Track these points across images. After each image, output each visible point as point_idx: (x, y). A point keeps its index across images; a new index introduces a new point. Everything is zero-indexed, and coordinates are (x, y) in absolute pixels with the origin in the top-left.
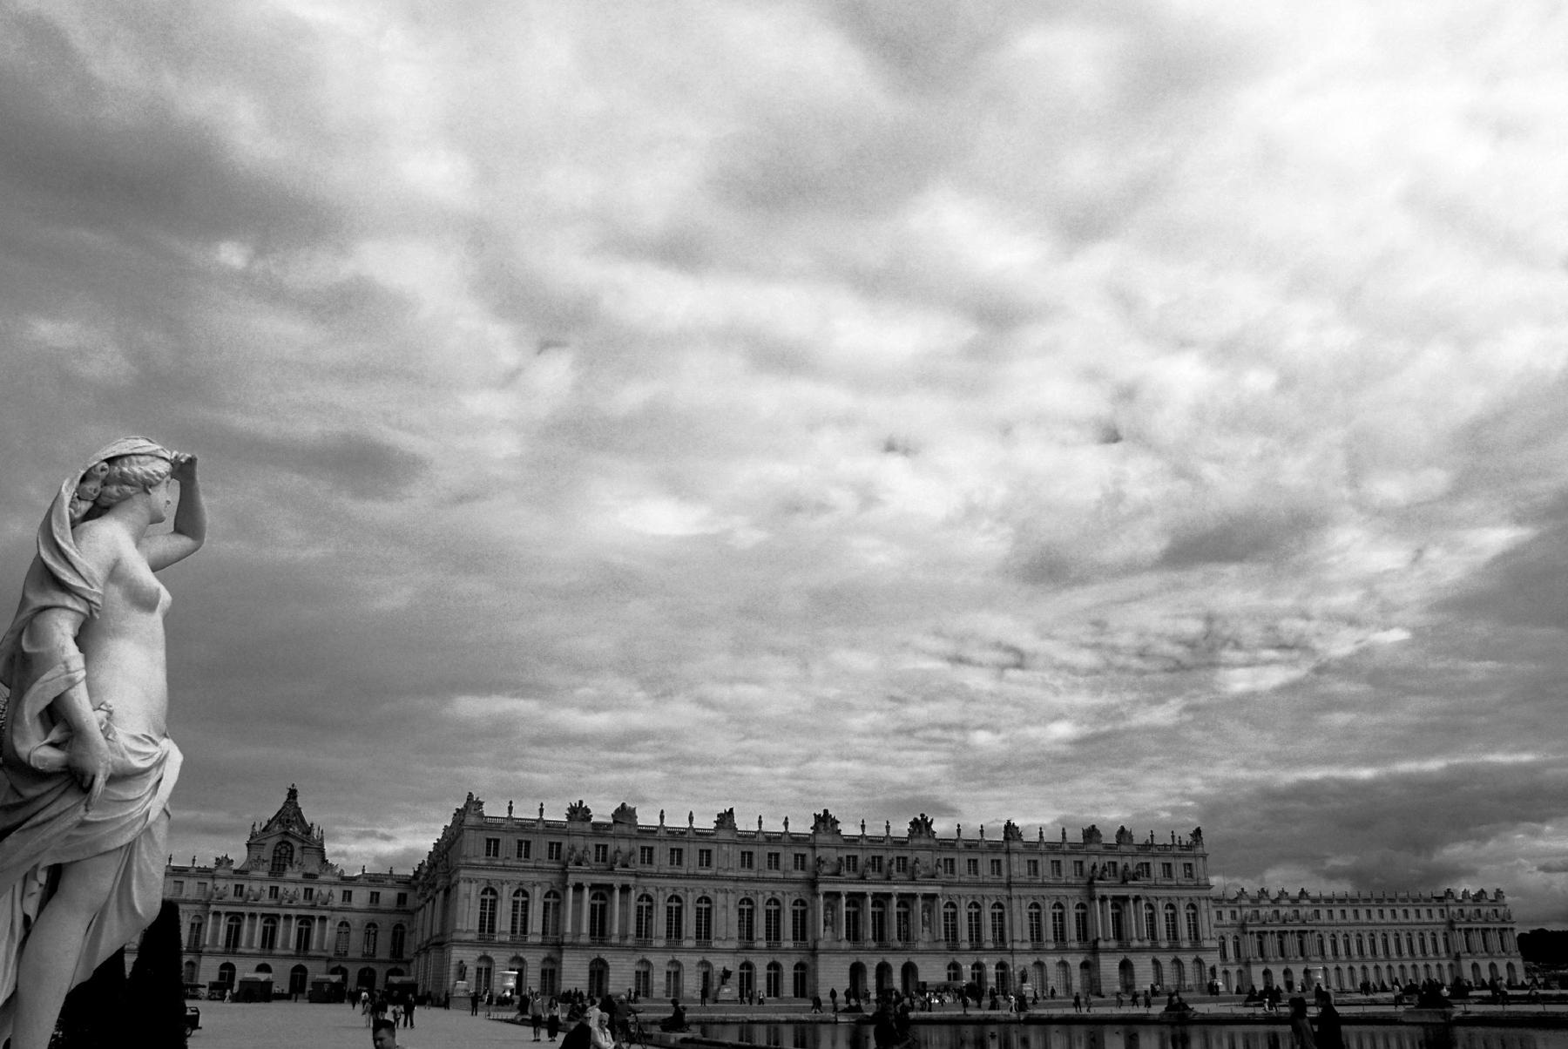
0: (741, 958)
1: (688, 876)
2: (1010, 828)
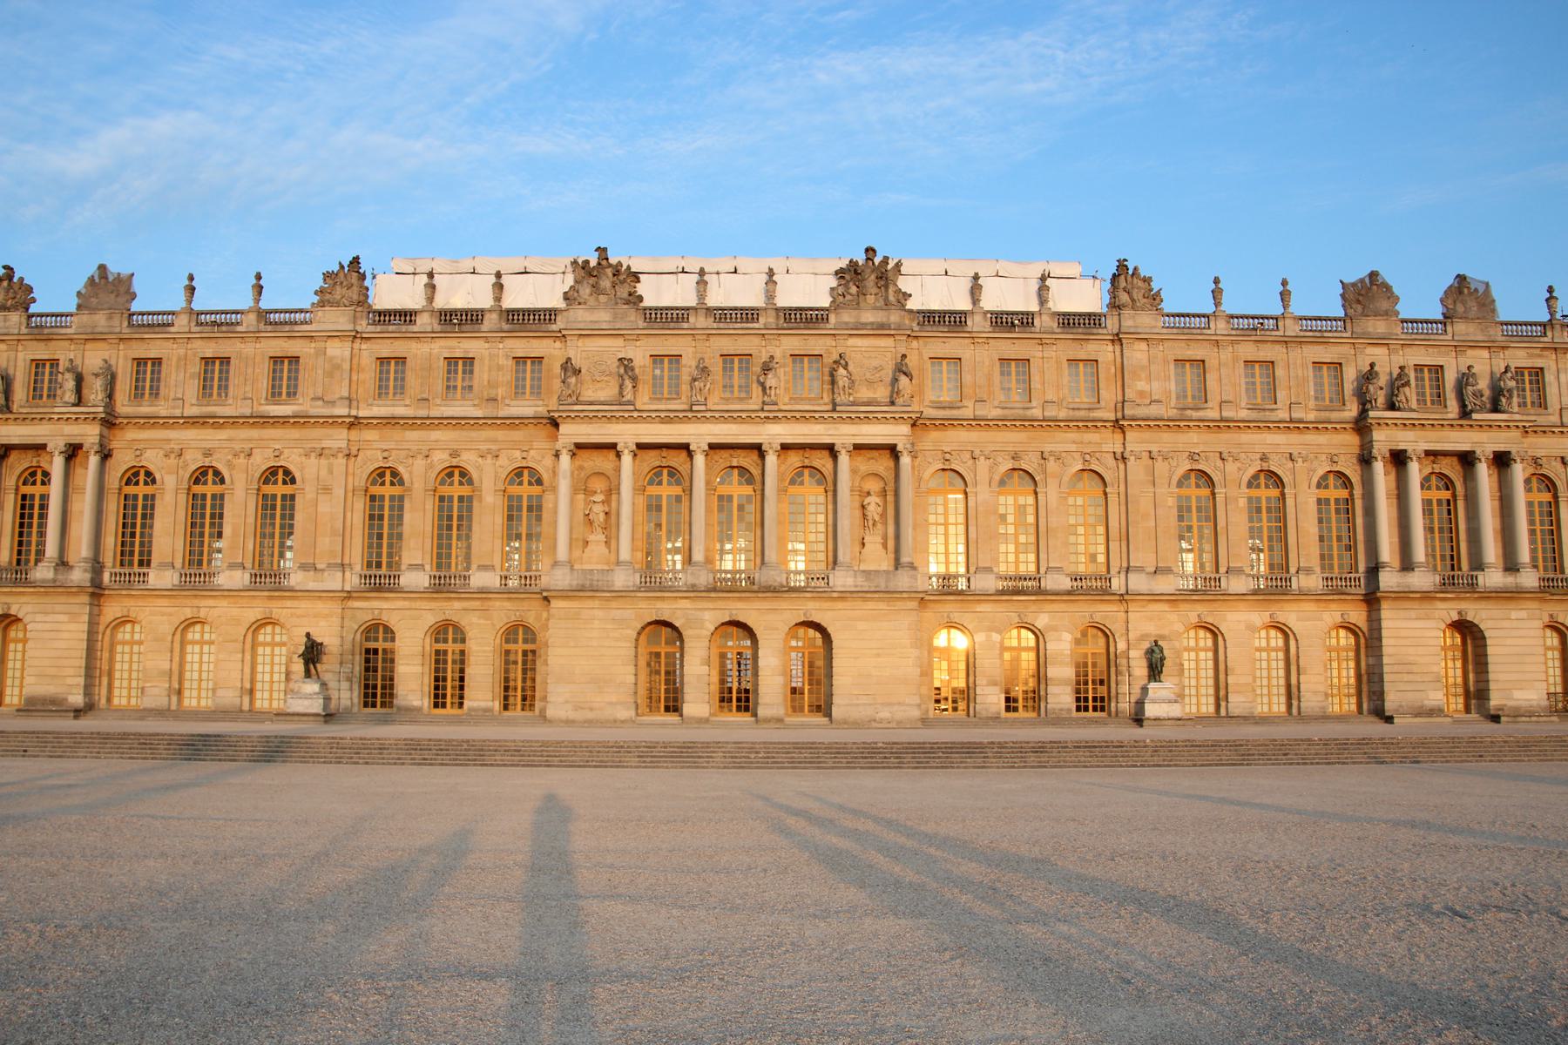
1: (233, 422)
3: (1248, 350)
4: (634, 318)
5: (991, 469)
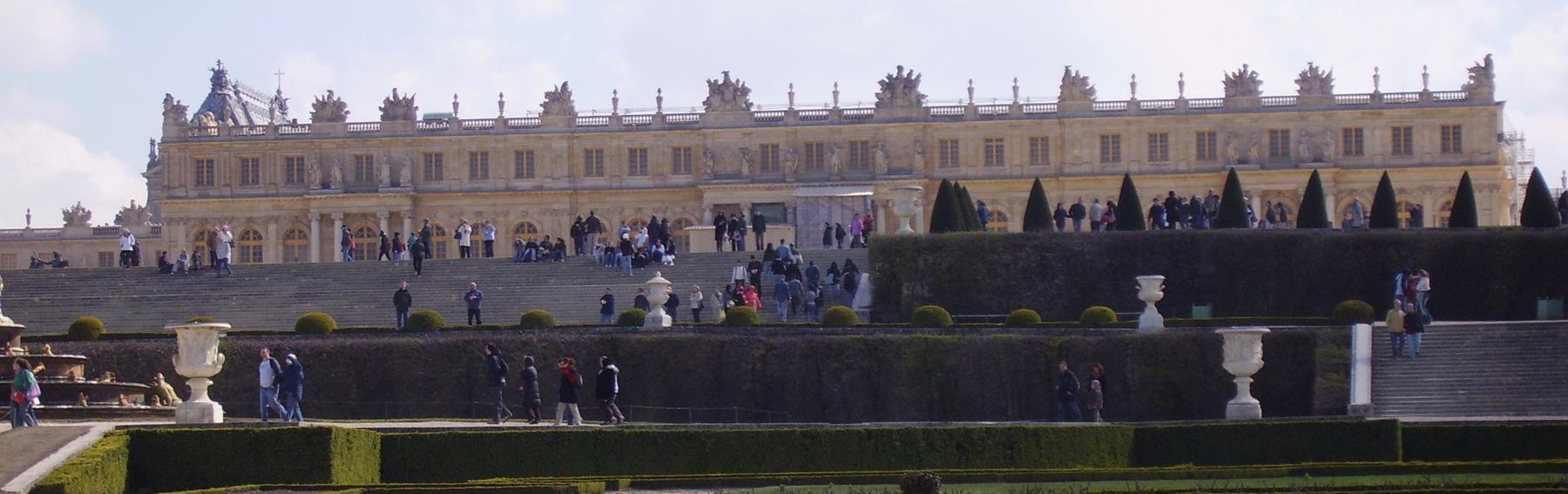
2: (1074, 85)
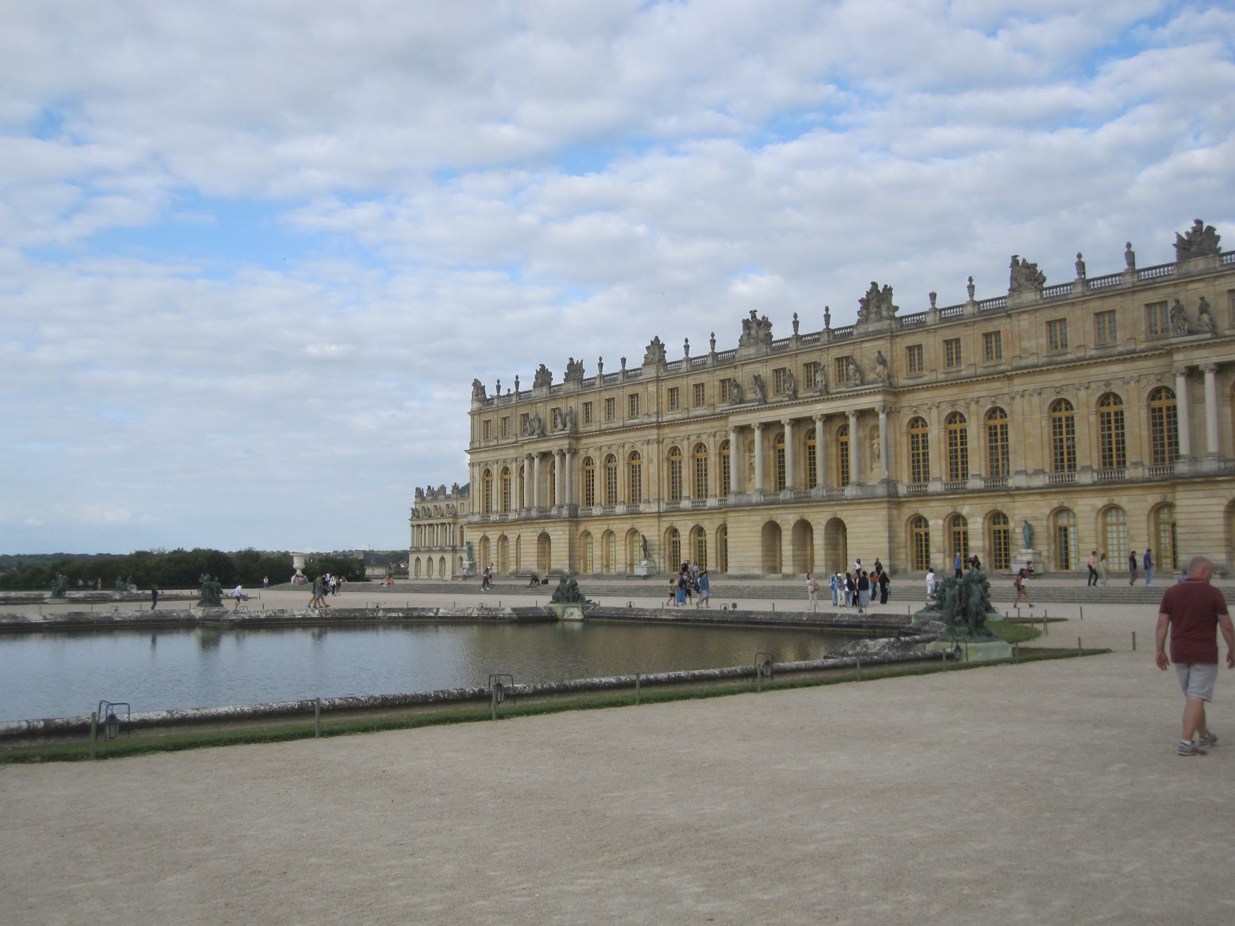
0: (665, 524)
2: (1025, 274)
3: (1098, 305)
4: (764, 349)
5: (939, 414)
